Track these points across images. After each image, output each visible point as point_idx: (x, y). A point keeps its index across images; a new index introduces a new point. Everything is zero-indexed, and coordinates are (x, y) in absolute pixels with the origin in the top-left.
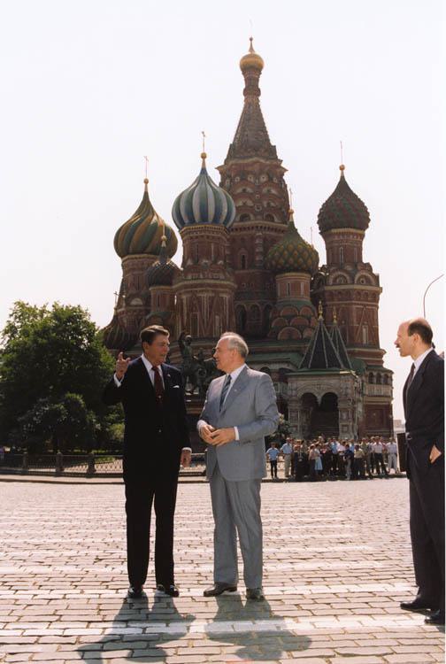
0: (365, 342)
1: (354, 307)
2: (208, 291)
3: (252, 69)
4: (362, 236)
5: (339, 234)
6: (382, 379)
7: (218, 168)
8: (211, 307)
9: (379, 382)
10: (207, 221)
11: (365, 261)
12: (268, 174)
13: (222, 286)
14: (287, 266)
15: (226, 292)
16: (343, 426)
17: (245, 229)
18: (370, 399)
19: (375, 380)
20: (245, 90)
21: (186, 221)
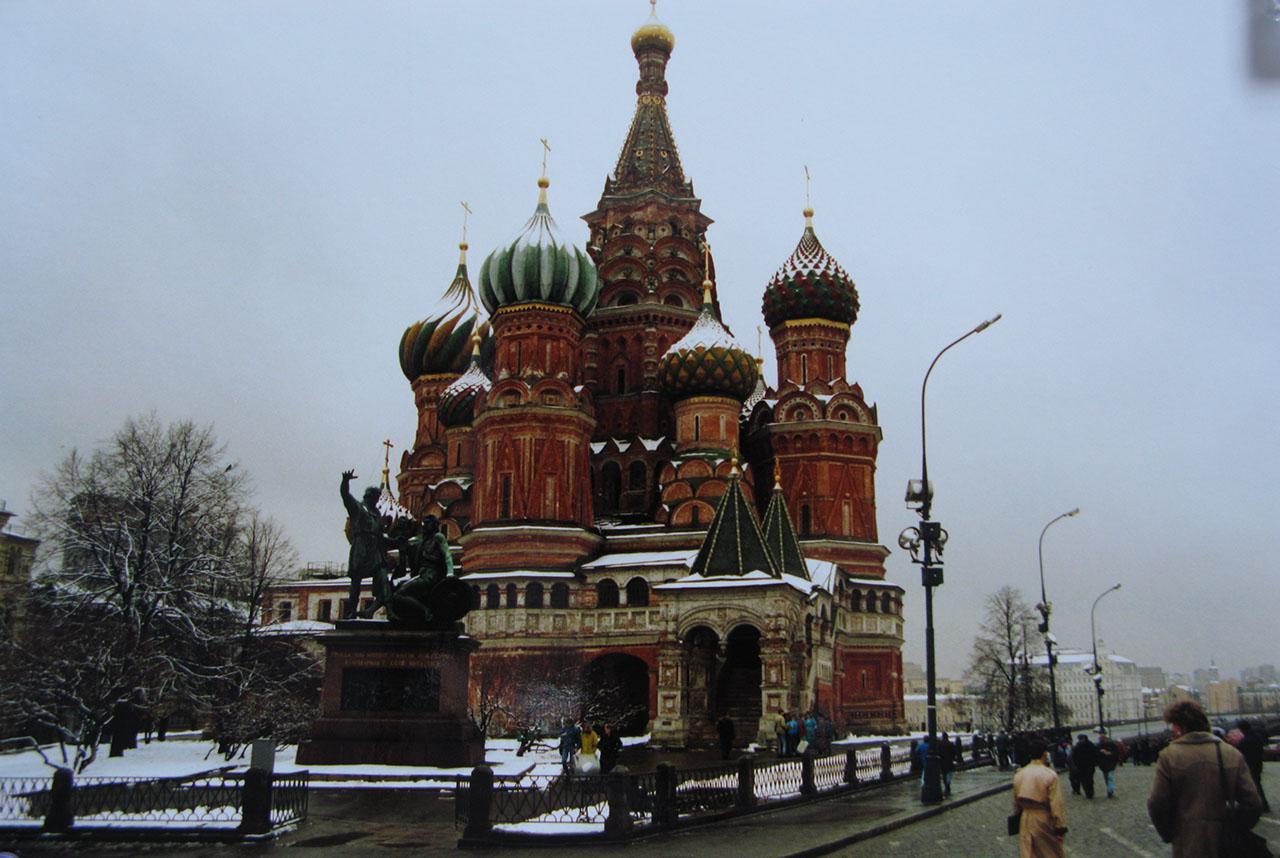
0: (846, 531)
1: (824, 466)
2: (533, 429)
3: (652, 50)
4: (846, 335)
5: (798, 330)
6: (878, 604)
7: (585, 218)
8: (536, 461)
9: (871, 609)
10: (539, 296)
11: (850, 381)
12: (671, 224)
13: (560, 419)
14: (693, 382)
15: (570, 432)
16: (770, 696)
17: (625, 321)
18: (854, 642)
19: (864, 605)
20: (639, 84)
21: (500, 297)
